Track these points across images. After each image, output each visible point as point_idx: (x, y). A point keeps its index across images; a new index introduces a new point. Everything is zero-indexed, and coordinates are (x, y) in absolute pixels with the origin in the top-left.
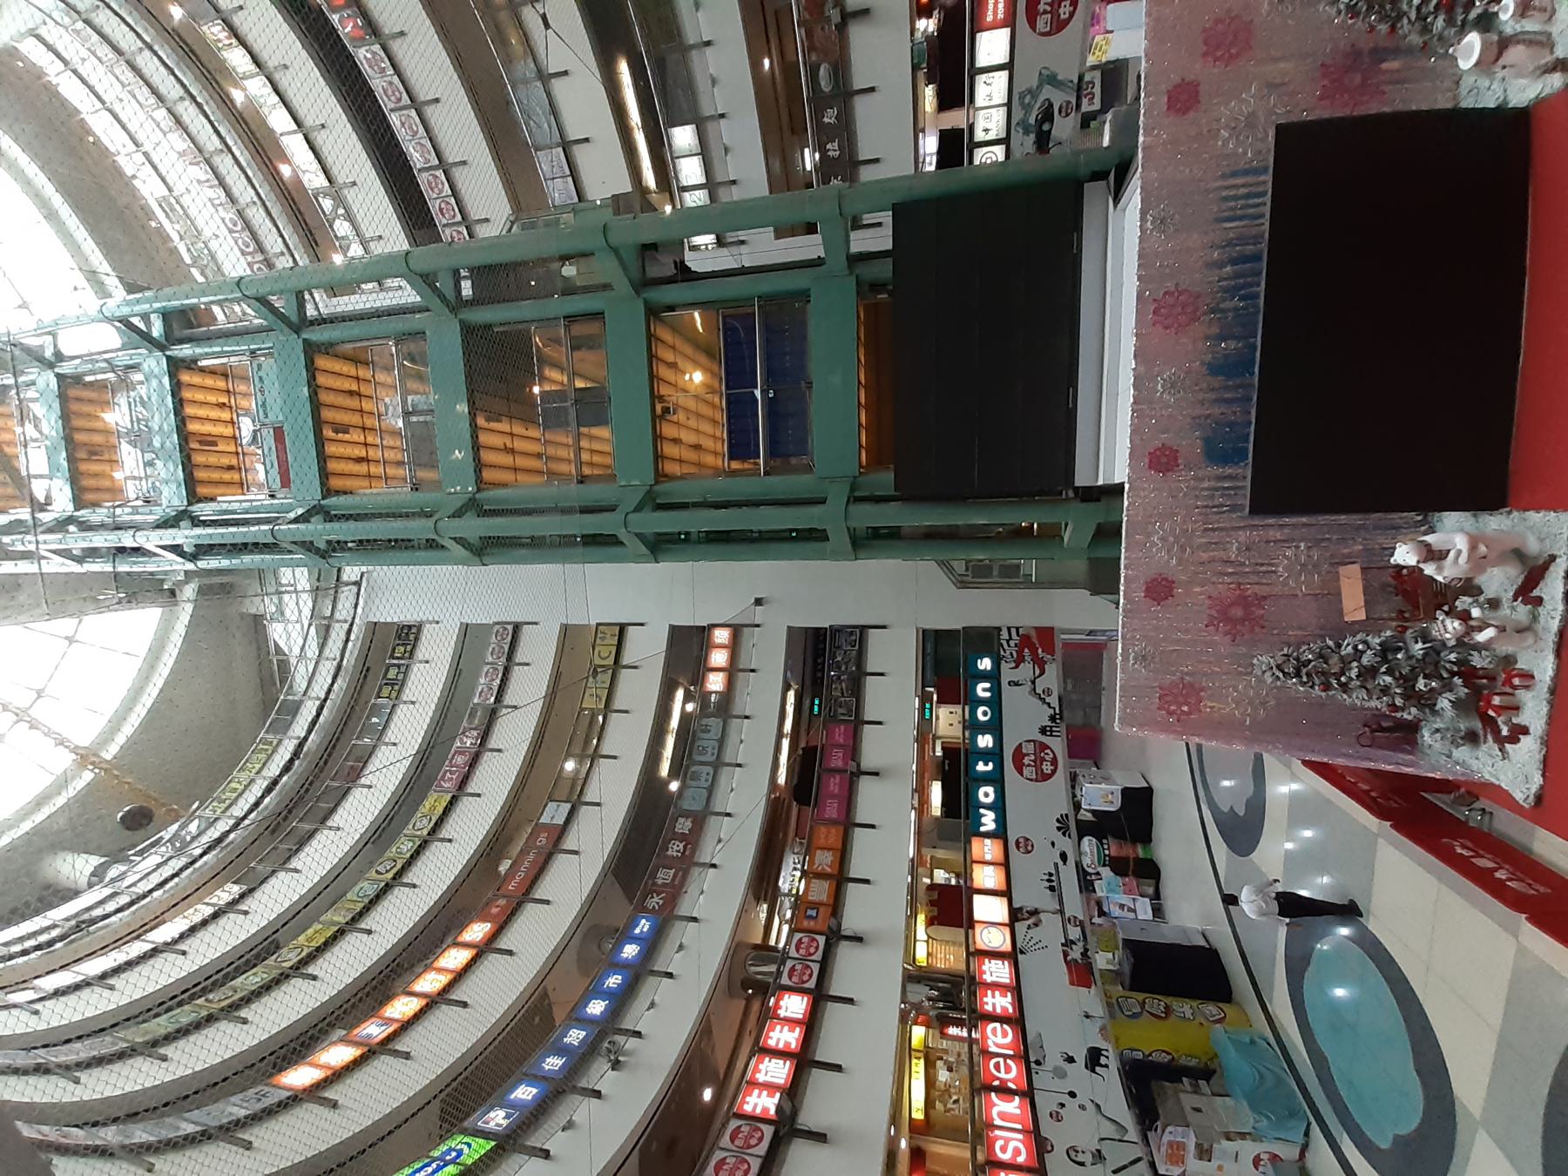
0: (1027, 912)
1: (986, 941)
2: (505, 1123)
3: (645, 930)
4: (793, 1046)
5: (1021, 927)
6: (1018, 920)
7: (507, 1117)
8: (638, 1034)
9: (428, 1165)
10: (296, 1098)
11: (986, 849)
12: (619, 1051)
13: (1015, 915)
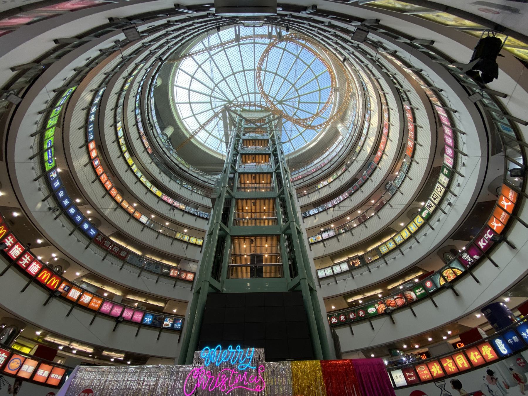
0: (18, 387)
1: (14, 360)
2: (51, 176)
3: (91, 232)
4: (20, 262)
5: (12, 381)
6: (16, 381)
7: (52, 177)
8: (55, 219)
9: (51, 155)
10: (87, 142)
11: (57, 376)
12: (54, 211)
13: (19, 380)
